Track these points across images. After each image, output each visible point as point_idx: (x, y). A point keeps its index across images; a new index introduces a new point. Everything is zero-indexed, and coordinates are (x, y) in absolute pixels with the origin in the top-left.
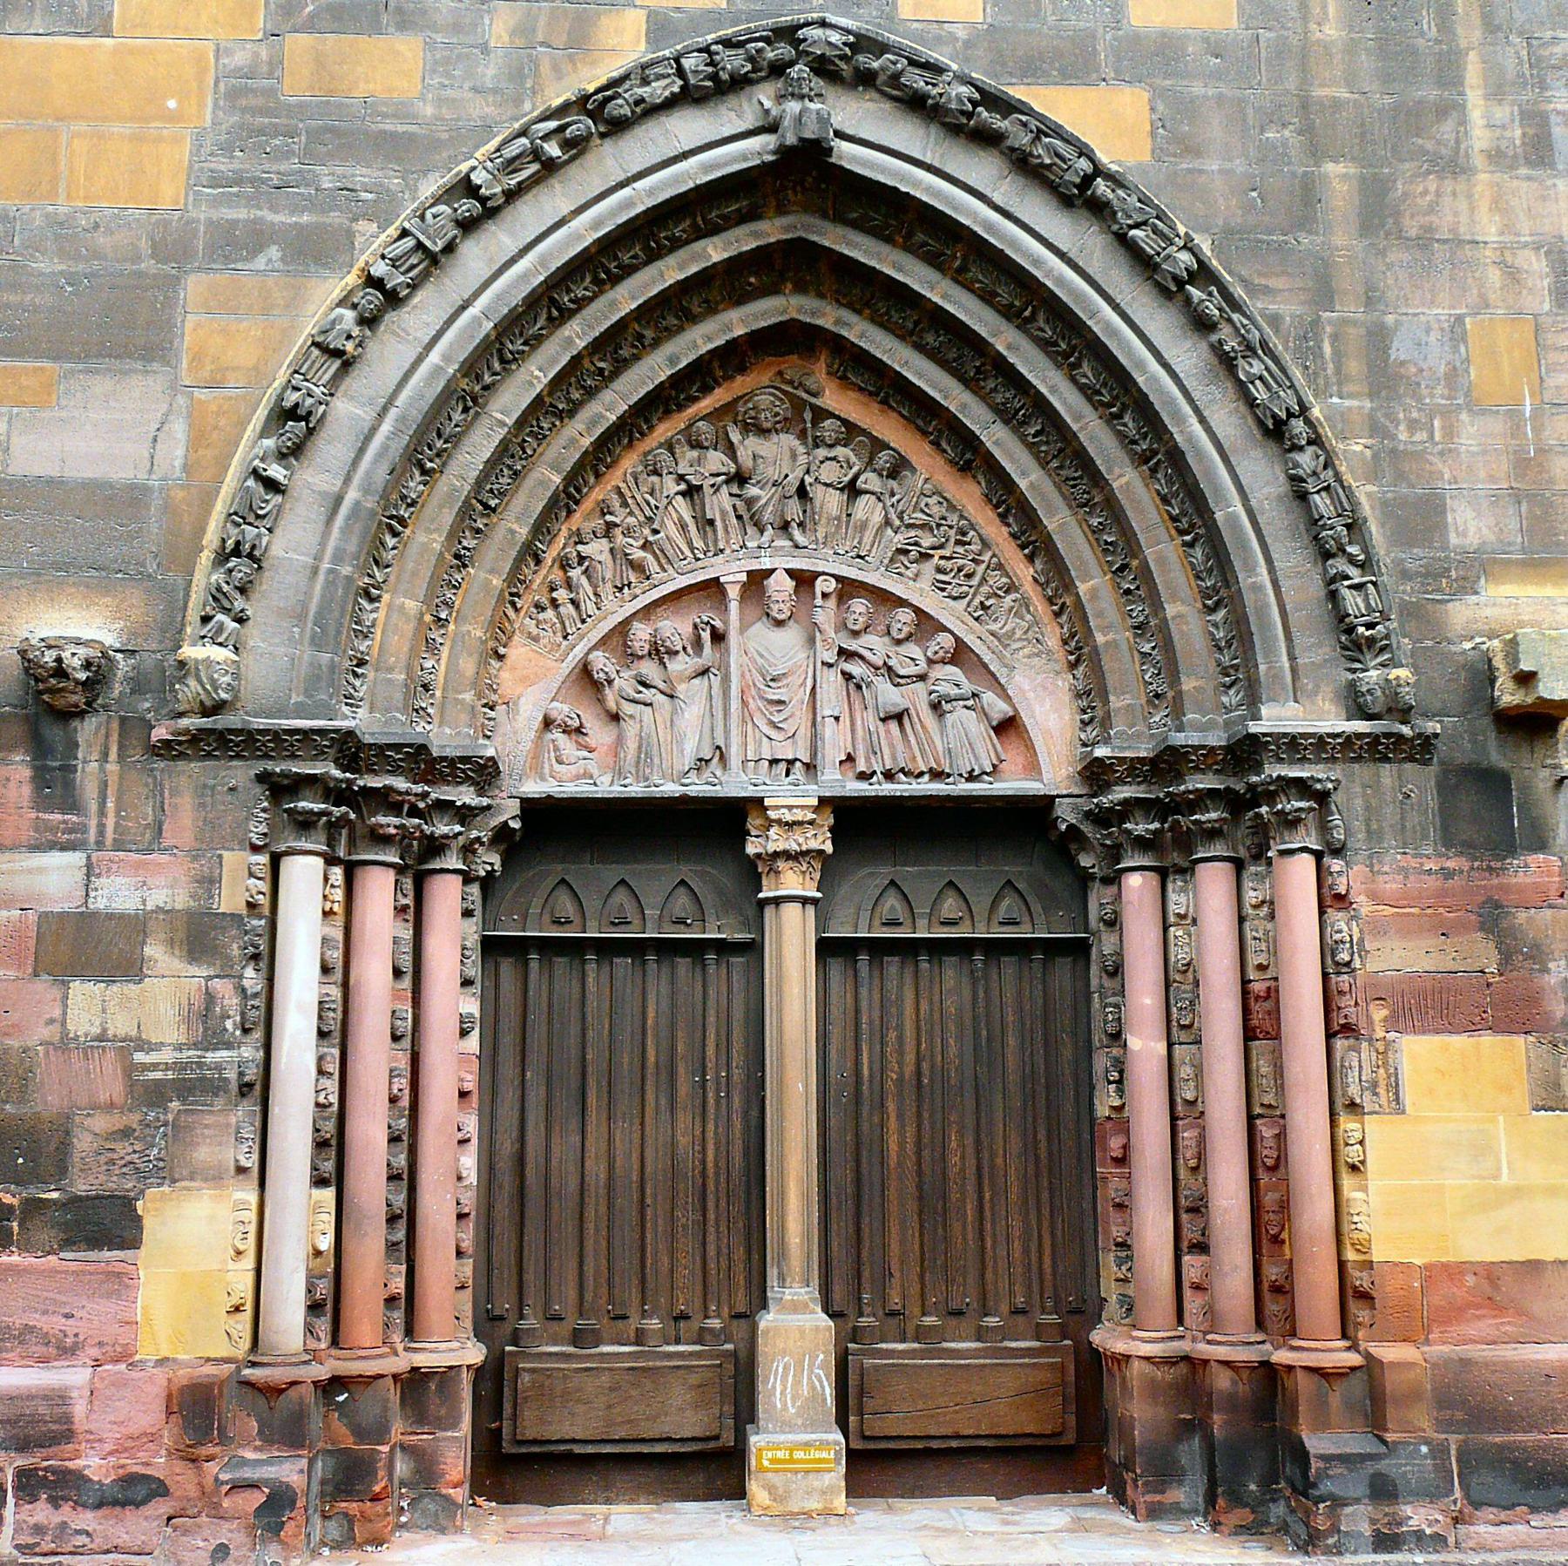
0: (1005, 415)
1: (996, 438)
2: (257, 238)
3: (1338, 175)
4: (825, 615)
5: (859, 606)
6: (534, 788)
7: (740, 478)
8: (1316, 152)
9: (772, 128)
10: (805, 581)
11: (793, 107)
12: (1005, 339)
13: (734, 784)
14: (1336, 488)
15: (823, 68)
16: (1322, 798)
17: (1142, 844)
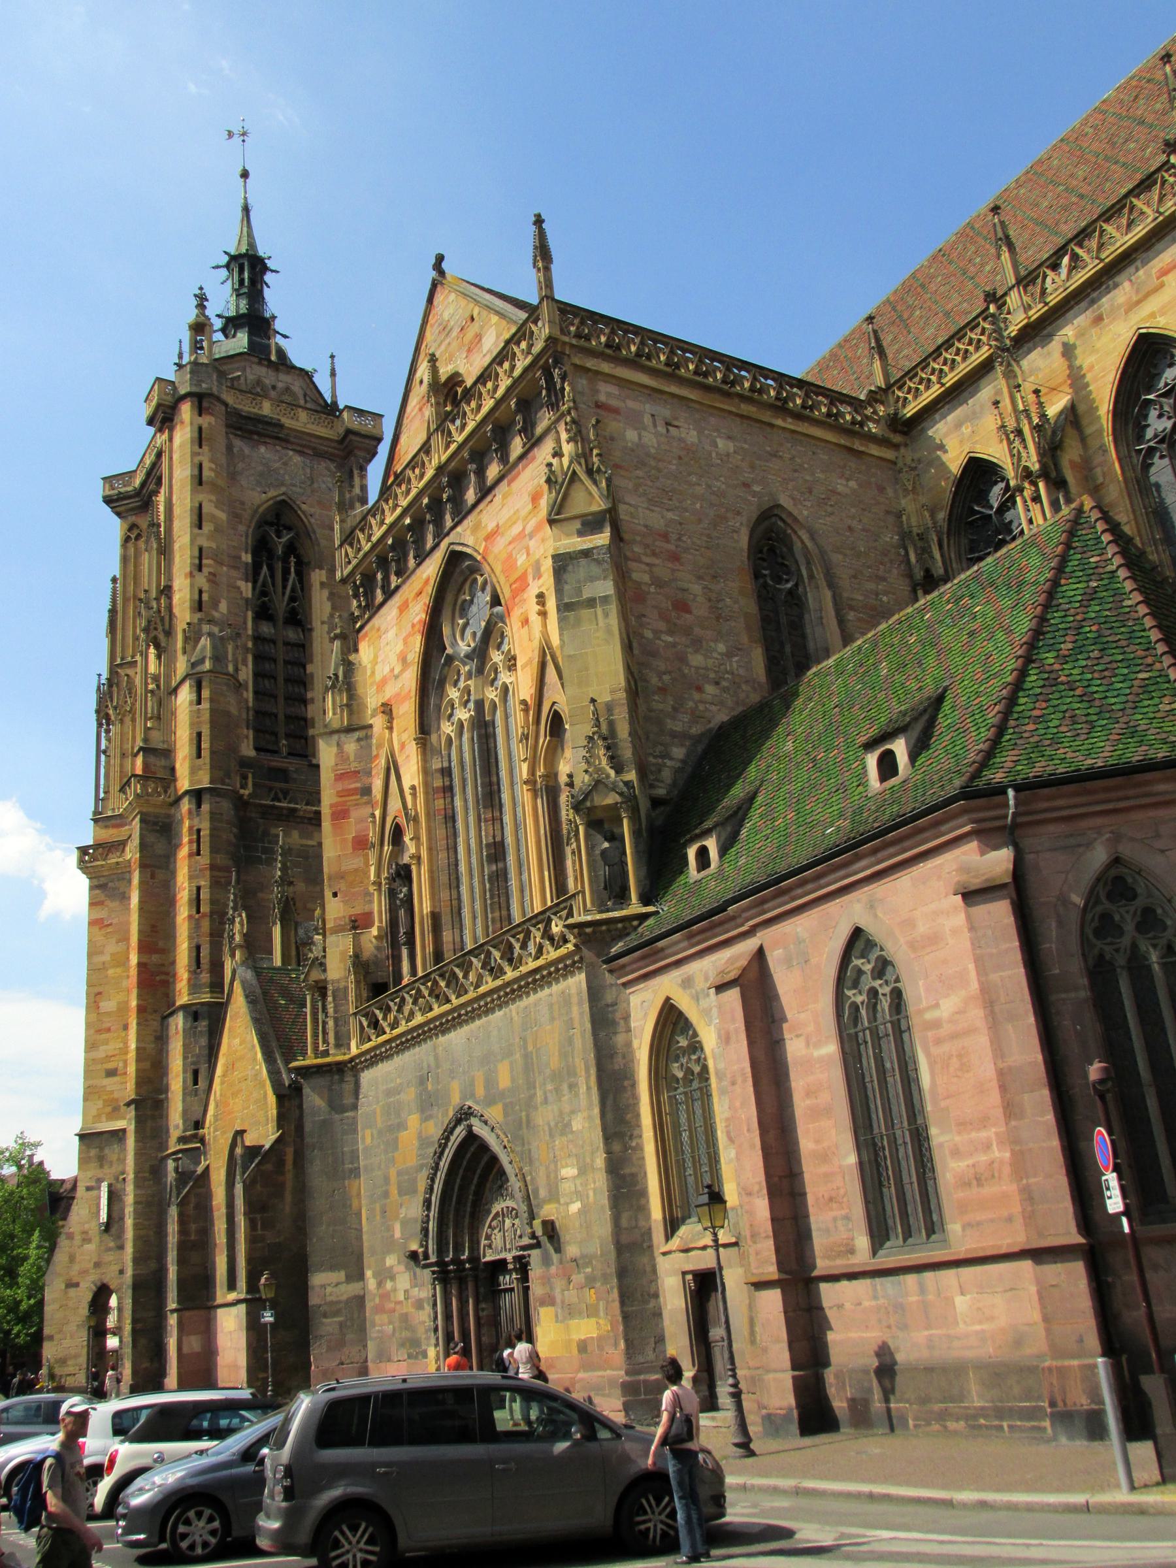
3: (524, 1114)
15: (465, 1114)
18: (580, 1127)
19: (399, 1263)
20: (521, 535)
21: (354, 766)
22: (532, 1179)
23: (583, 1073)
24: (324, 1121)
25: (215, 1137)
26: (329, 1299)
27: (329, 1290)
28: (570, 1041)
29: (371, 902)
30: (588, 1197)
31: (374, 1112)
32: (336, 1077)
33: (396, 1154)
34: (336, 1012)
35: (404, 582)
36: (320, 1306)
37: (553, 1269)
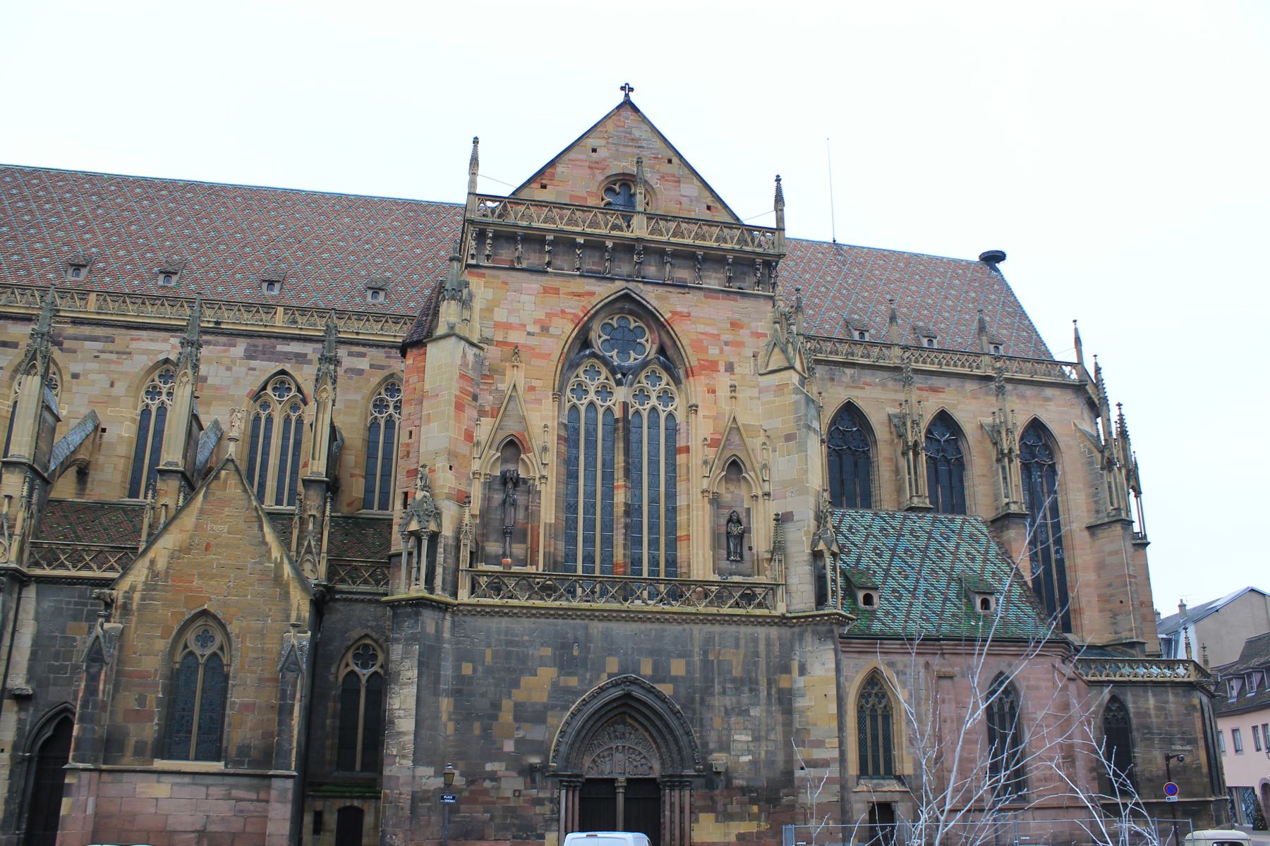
0: (652, 725)
1: (651, 728)
2: (556, 706)
4: (626, 752)
5: (631, 751)
6: (587, 777)
7: (615, 731)
8: (695, 693)
9: (624, 690)
10: (624, 747)
11: (626, 688)
12: (653, 717)
13: (614, 776)
14: (694, 742)
16: (691, 782)
17: (669, 786)
18: (758, 715)
19: (507, 769)
20: (717, 336)
21: (471, 373)
22: (701, 737)
23: (765, 684)
24: (431, 646)
25: (142, 607)
26: (424, 788)
27: (424, 780)
28: (756, 664)
29: (470, 485)
30: (759, 754)
31: (483, 655)
32: (441, 614)
33: (514, 691)
34: (445, 562)
35: (556, 275)
36: (418, 792)
37: (717, 792)
